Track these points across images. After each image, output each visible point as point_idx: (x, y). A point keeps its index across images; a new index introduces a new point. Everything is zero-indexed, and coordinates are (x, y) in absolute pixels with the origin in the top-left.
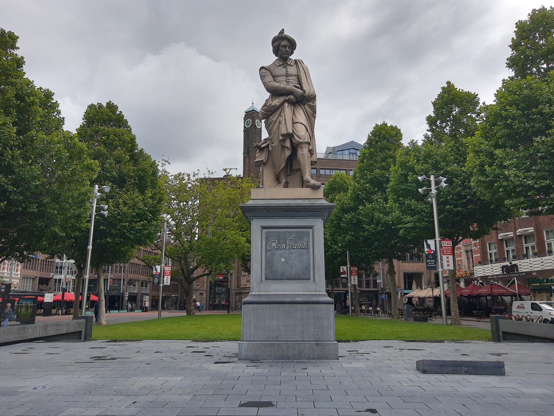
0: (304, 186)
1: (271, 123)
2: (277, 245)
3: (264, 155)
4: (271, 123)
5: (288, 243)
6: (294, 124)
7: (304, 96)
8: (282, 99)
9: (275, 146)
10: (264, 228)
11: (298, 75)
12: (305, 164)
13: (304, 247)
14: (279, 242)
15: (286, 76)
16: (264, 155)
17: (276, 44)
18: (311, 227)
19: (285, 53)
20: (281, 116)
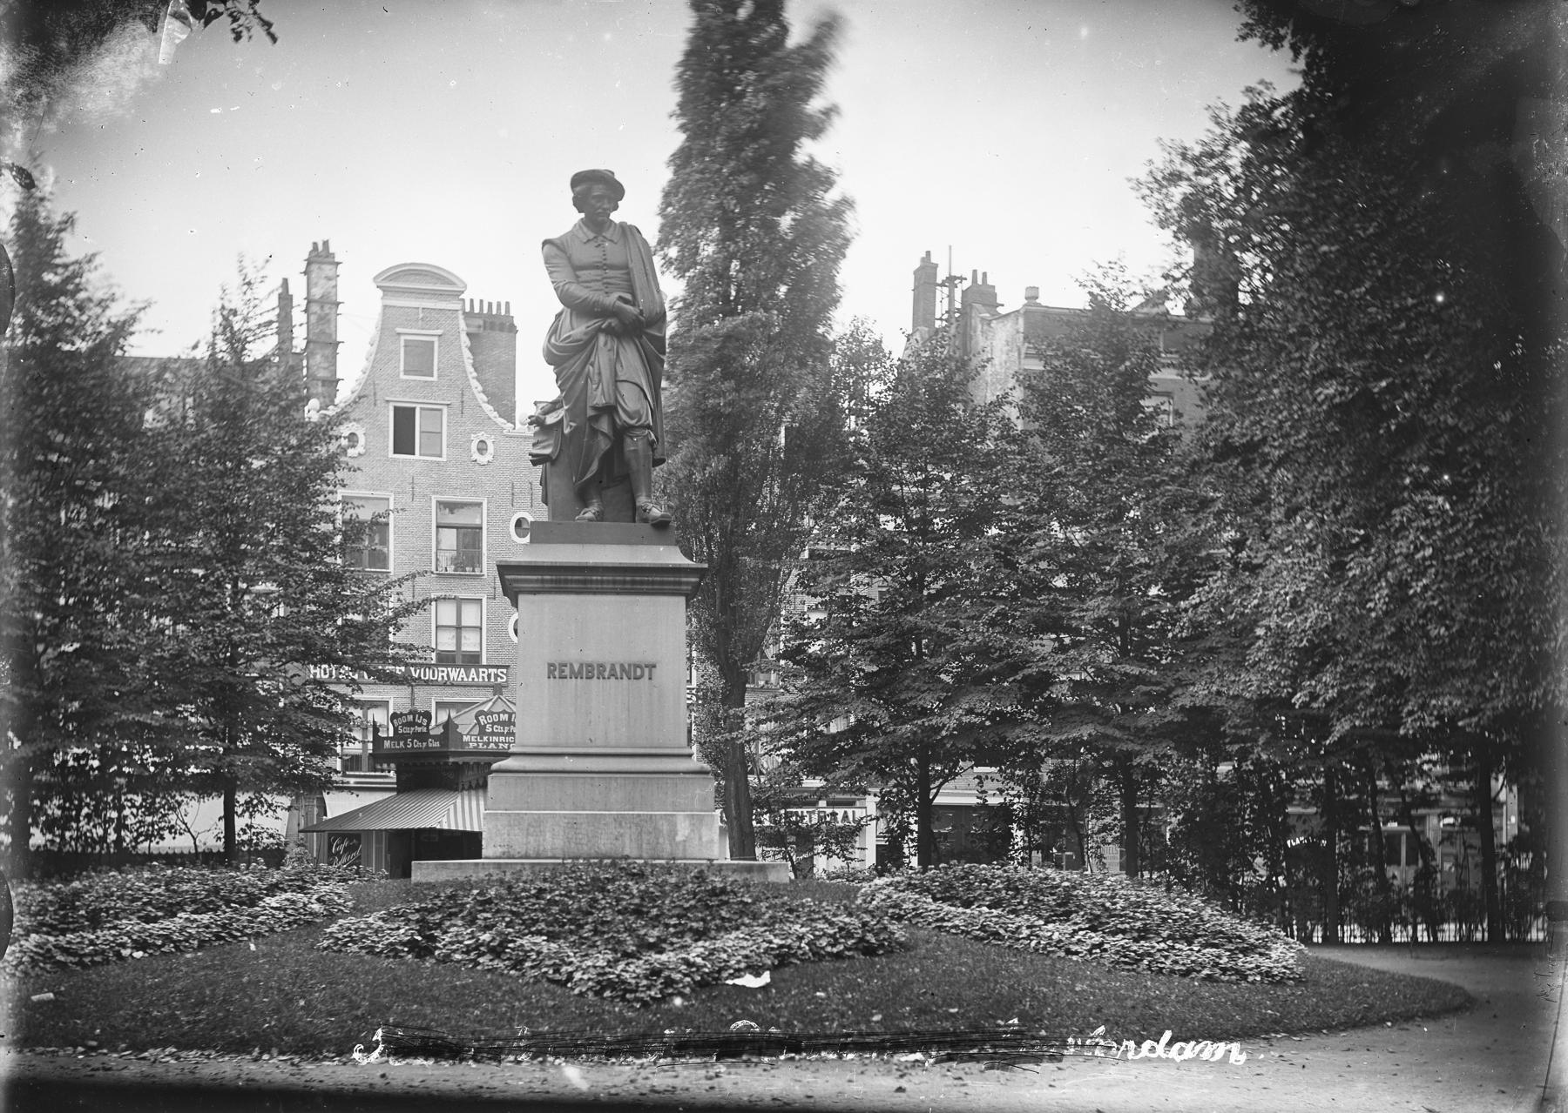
3: (551, 442)
7: (639, 320)
8: (594, 323)
9: (576, 428)
11: (626, 267)
16: (551, 442)
17: (578, 189)
20: (592, 365)
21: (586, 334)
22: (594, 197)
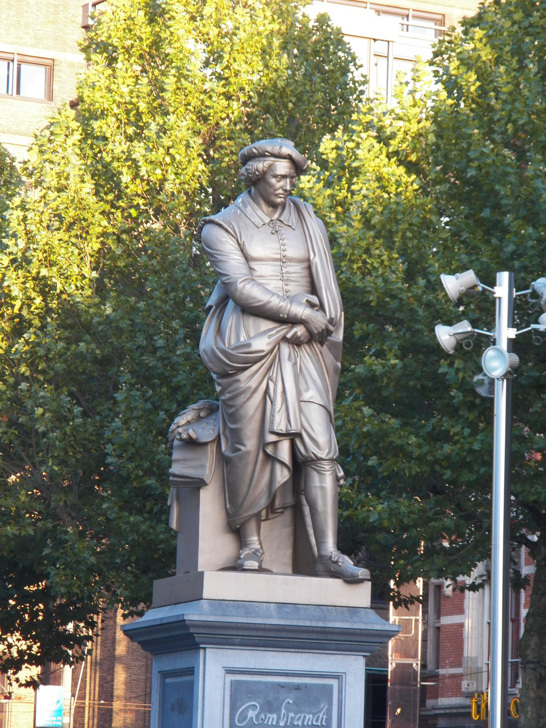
0: (320, 568)
1: (244, 392)
2: (257, 716)
4: (244, 392)
5: (283, 711)
10: (230, 671)
11: (309, 260)
12: (326, 512)
13: (319, 724)
14: (262, 710)
15: (280, 260)
18: (337, 677)
21: (268, 344)
22: (275, 176)
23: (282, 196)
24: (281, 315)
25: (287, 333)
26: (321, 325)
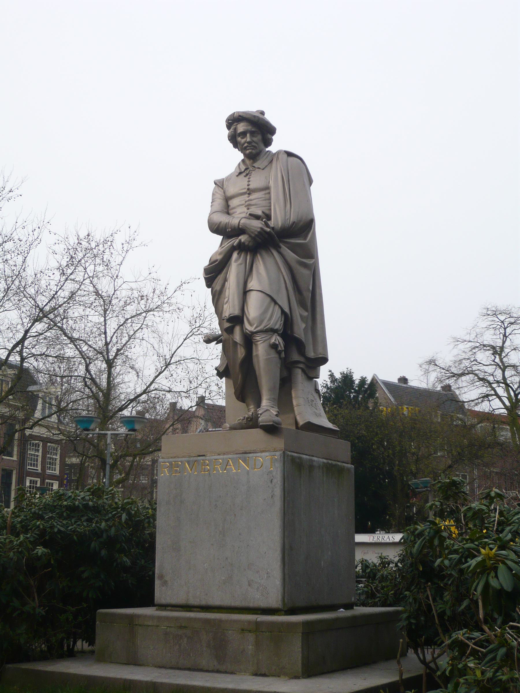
6: (248, 294)
19: (247, 146)
21: (220, 254)
23: (248, 148)
24: (228, 230)
25: (235, 242)
26: (256, 229)
